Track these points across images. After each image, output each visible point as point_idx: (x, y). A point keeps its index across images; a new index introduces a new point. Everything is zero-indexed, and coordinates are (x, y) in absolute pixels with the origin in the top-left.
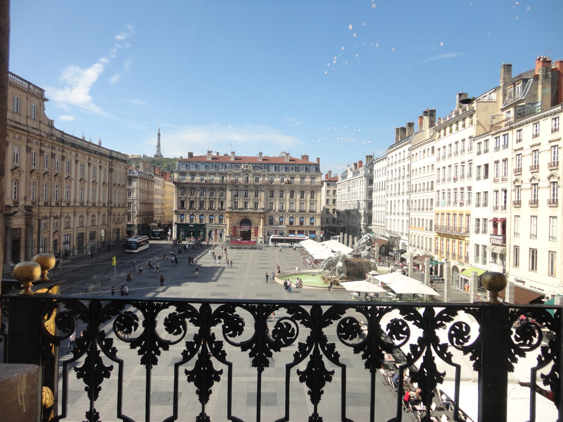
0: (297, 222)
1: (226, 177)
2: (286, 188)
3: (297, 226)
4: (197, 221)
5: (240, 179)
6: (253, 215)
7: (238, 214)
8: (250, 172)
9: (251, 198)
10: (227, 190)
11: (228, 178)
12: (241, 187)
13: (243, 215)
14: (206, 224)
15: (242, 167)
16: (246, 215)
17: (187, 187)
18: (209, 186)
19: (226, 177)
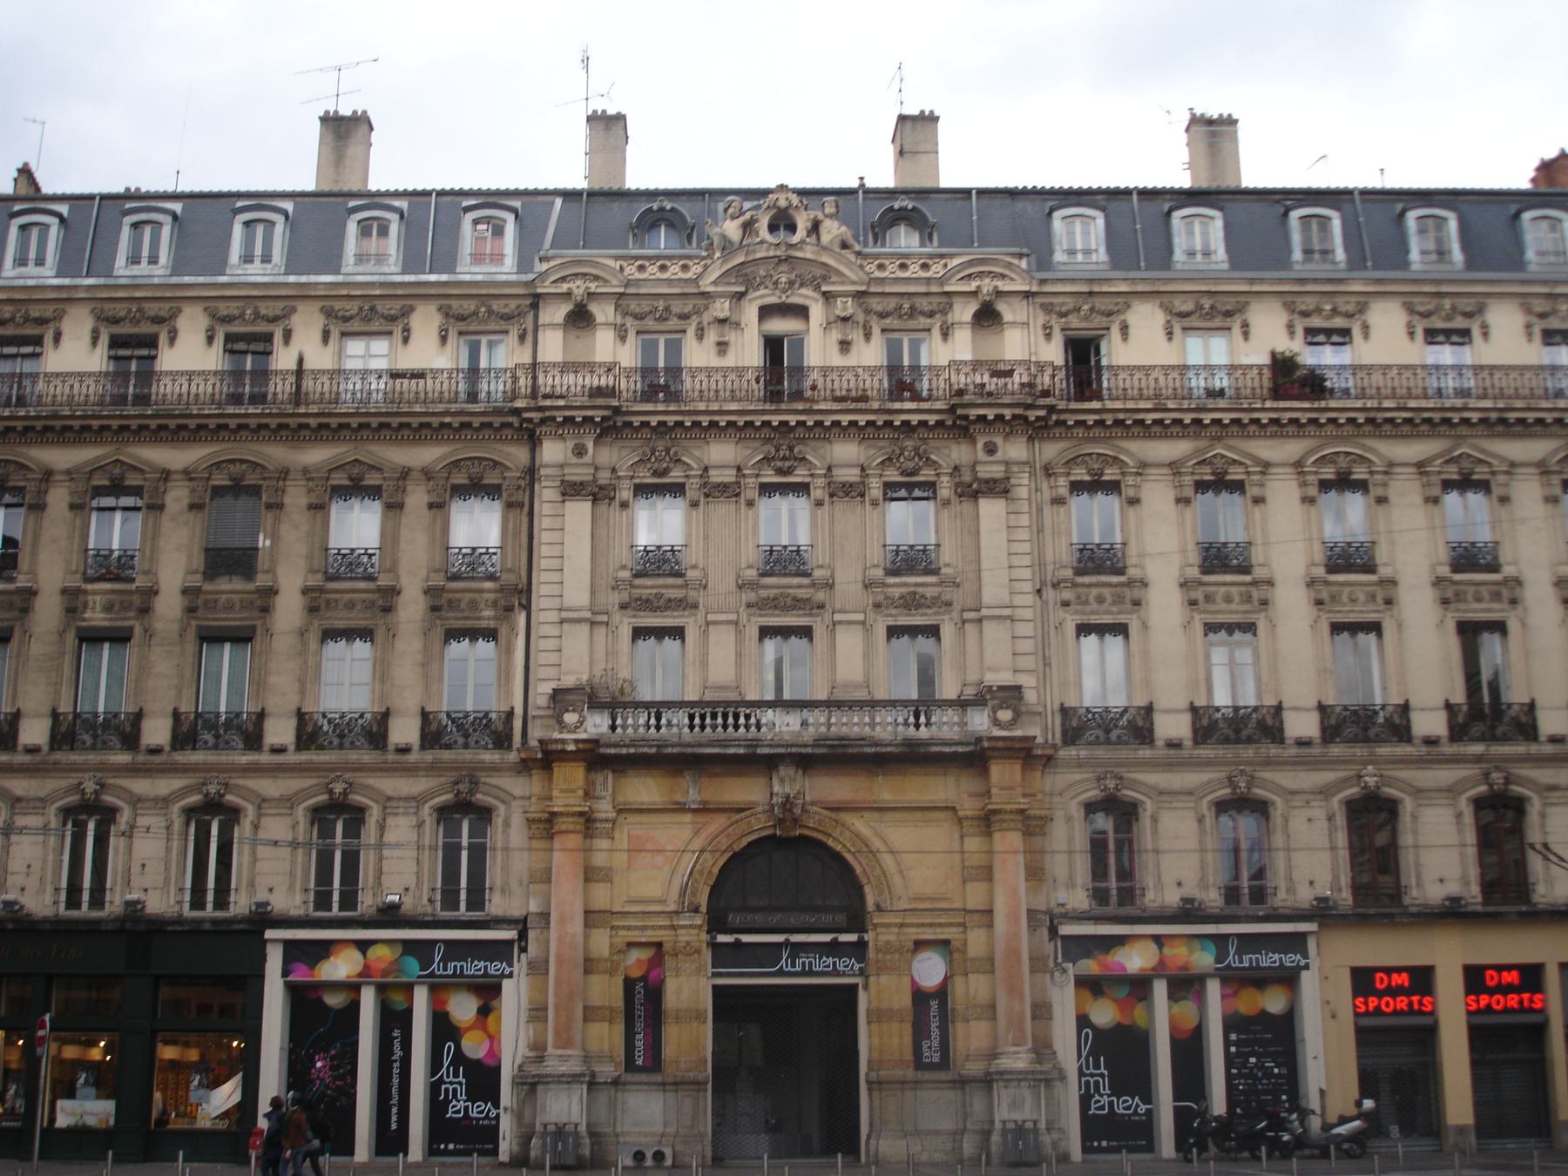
0: (1440, 855)
1: (528, 337)
2: (1266, 449)
3: (1452, 914)
4: (149, 872)
5: (697, 354)
6: (885, 789)
7: (691, 790)
8: (817, 277)
9: (848, 581)
10: (547, 493)
11: (552, 346)
12: (721, 454)
13: (747, 790)
14: (263, 918)
15: (732, 229)
16: (786, 784)
17: (48, 475)
18: (317, 455)
19: (528, 337)
